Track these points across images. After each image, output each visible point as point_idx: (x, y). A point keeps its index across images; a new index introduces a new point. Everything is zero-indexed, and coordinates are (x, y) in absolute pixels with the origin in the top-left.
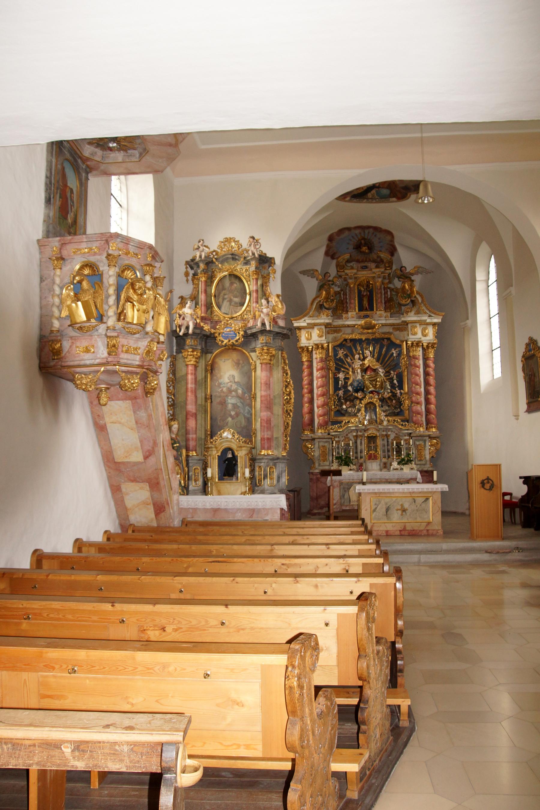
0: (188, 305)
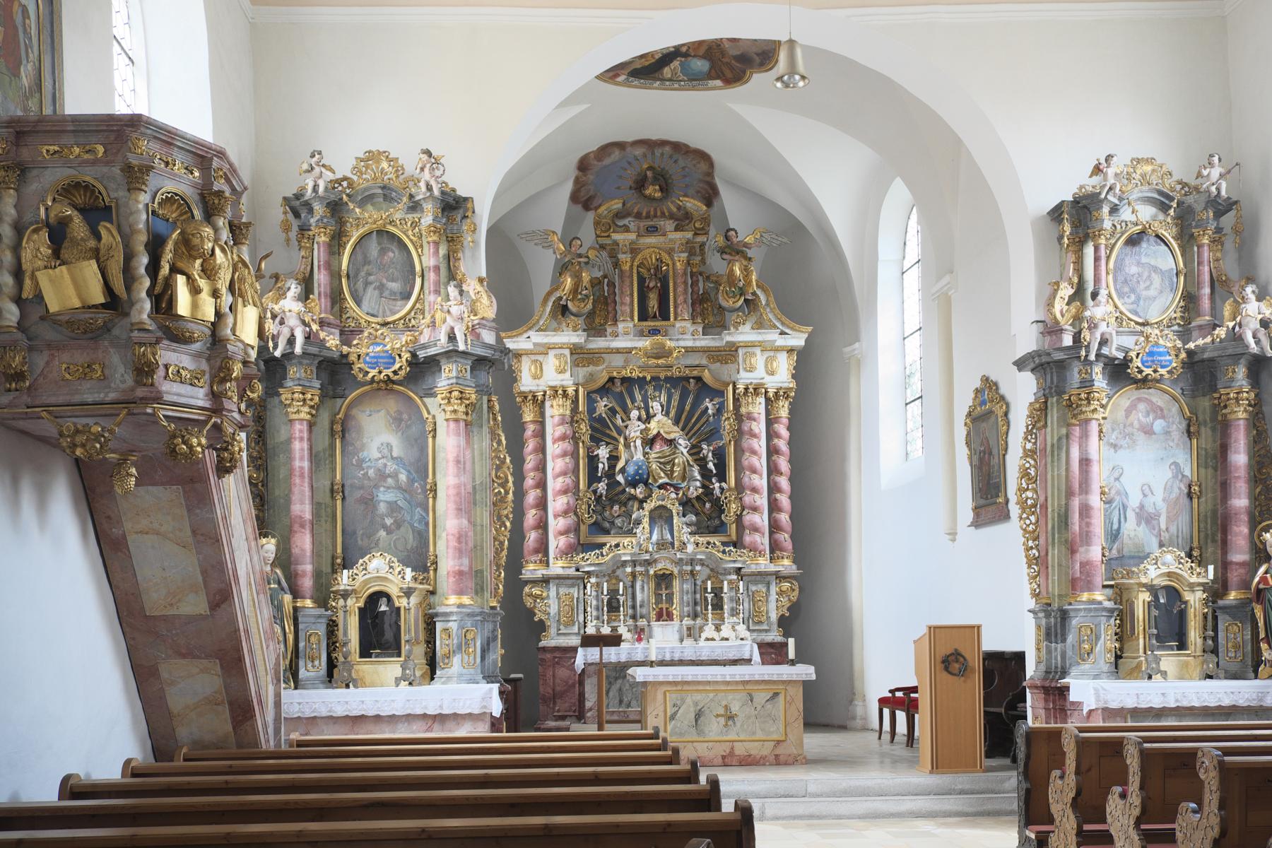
0: (290, 294)
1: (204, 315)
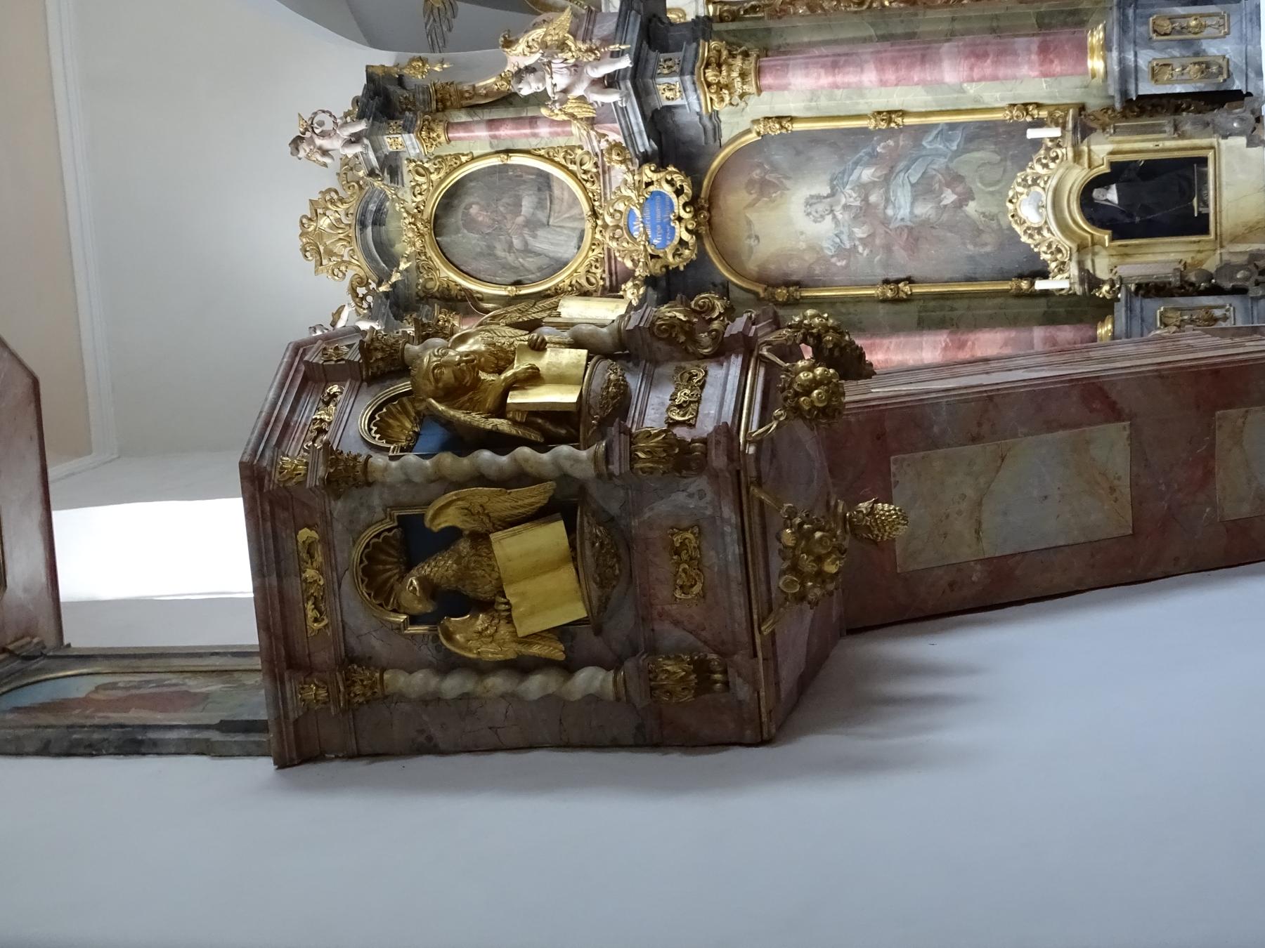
1: (576, 365)
